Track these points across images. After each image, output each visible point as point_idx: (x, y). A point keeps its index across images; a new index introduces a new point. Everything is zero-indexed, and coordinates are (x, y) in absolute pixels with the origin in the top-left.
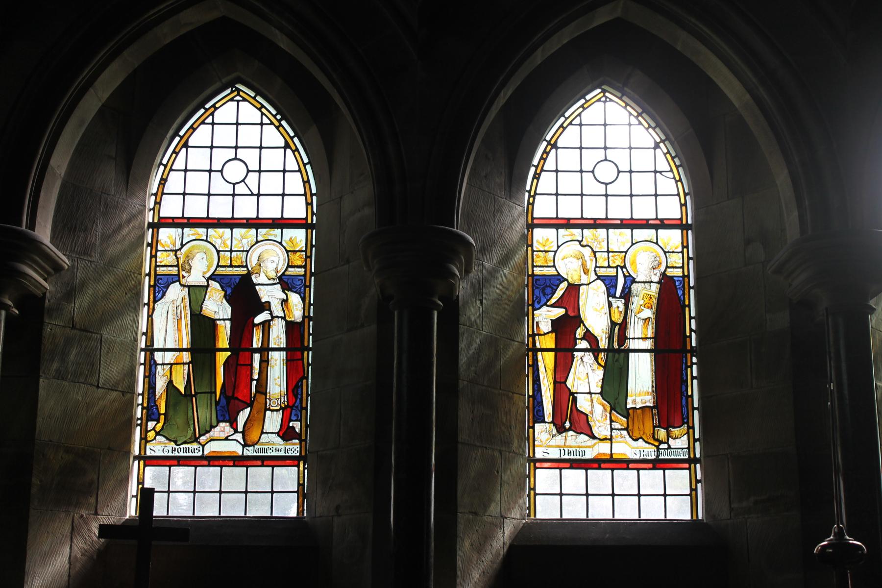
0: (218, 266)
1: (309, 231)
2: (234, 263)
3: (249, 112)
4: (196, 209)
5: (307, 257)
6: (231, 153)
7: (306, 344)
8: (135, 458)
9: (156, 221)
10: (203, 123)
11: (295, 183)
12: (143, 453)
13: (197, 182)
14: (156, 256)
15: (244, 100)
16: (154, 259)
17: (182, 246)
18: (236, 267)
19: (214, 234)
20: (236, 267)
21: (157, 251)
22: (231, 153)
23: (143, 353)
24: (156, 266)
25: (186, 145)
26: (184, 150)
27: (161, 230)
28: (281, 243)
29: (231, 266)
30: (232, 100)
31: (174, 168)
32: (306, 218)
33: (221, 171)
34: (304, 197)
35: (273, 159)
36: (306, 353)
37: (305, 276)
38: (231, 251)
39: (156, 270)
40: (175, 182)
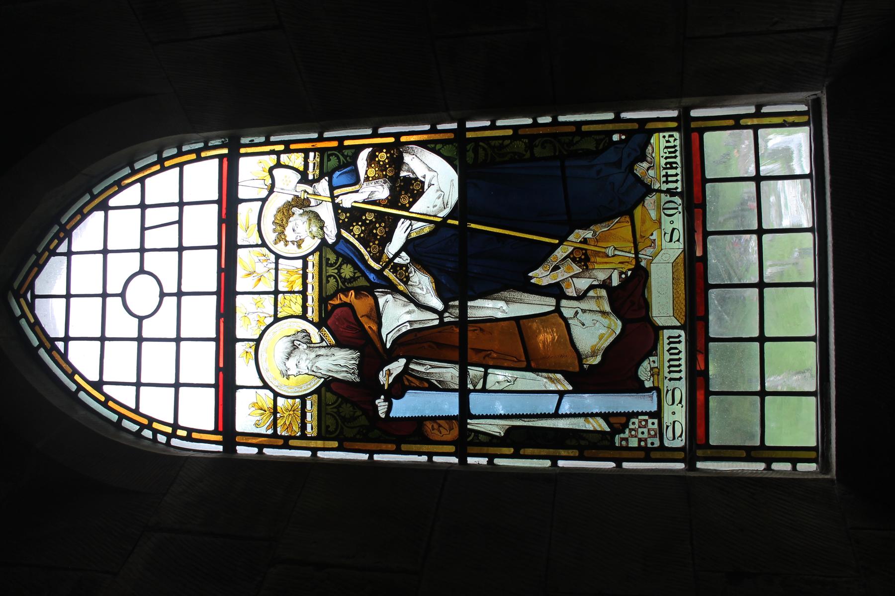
0: (303, 317)
1: (243, 151)
2: (298, 287)
3: (51, 278)
4: (201, 363)
5: (287, 151)
6: (114, 304)
7: (451, 136)
8: (691, 467)
9: (219, 438)
10: (65, 356)
11: (161, 186)
12: (682, 455)
13: (158, 363)
14: (286, 439)
15: (32, 287)
16: (292, 442)
17: (266, 386)
18: (305, 284)
19: (244, 328)
20: (305, 284)
21: (275, 435)
22: (114, 304)
23: (471, 460)
24: (304, 437)
25: (98, 385)
26: (107, 389)
27: (239, 428)
28: (264, 201)
29: (304, 293)
30: (32, 307)
31: (133, 407)
32: (220, 157)
33: (141, 319)
34: (186, 168)
35: (123, 226)
36: (469, 135)
37: (322, 151)
38: (276, 293)
39: (312, 438)
40: (157, 405)
